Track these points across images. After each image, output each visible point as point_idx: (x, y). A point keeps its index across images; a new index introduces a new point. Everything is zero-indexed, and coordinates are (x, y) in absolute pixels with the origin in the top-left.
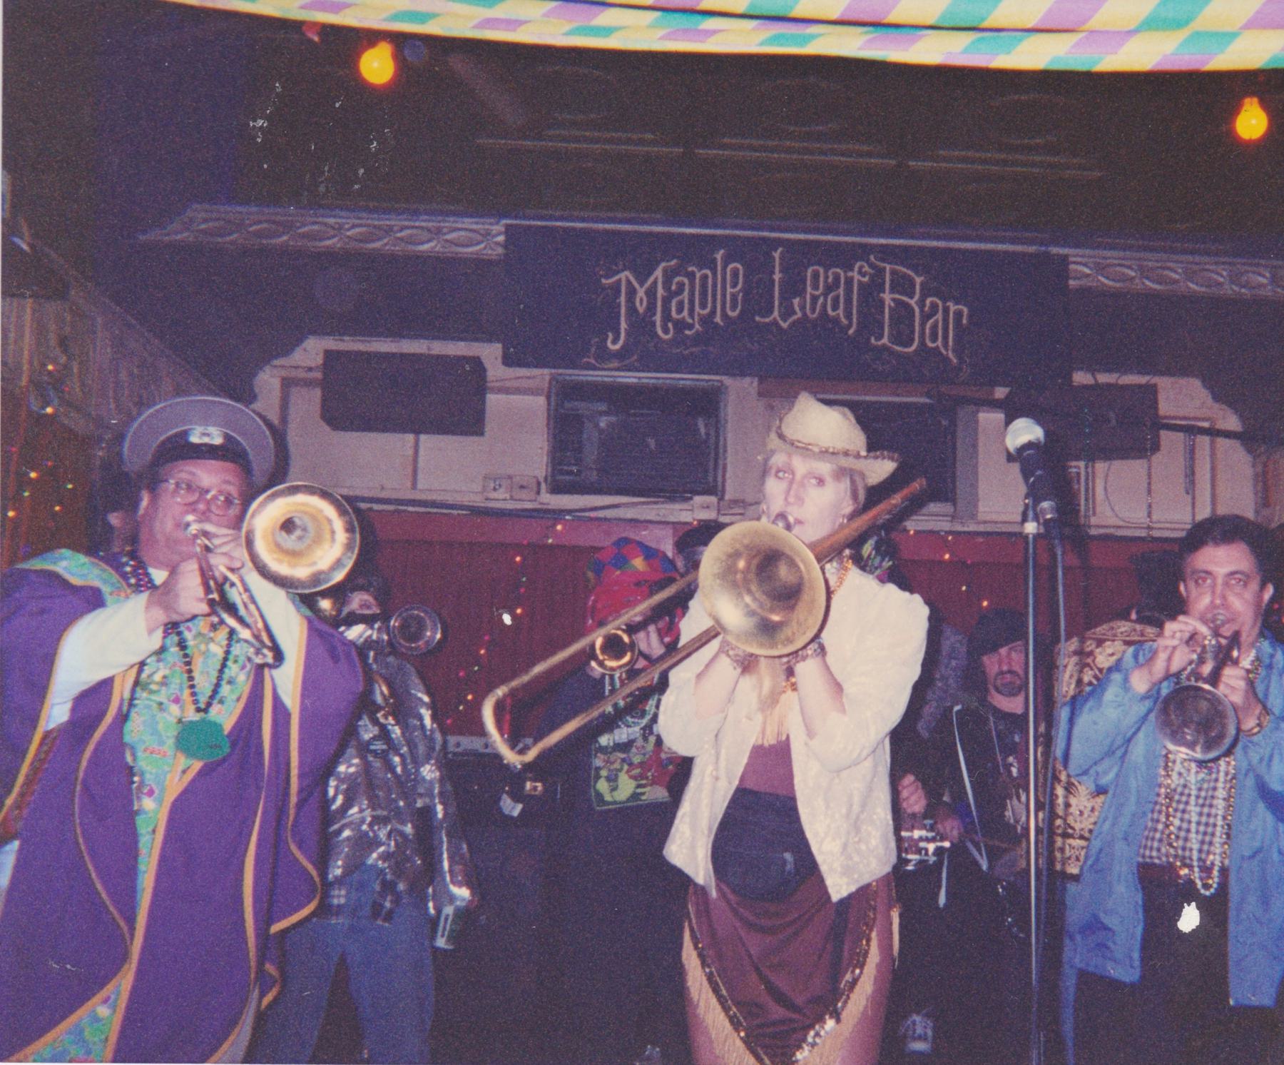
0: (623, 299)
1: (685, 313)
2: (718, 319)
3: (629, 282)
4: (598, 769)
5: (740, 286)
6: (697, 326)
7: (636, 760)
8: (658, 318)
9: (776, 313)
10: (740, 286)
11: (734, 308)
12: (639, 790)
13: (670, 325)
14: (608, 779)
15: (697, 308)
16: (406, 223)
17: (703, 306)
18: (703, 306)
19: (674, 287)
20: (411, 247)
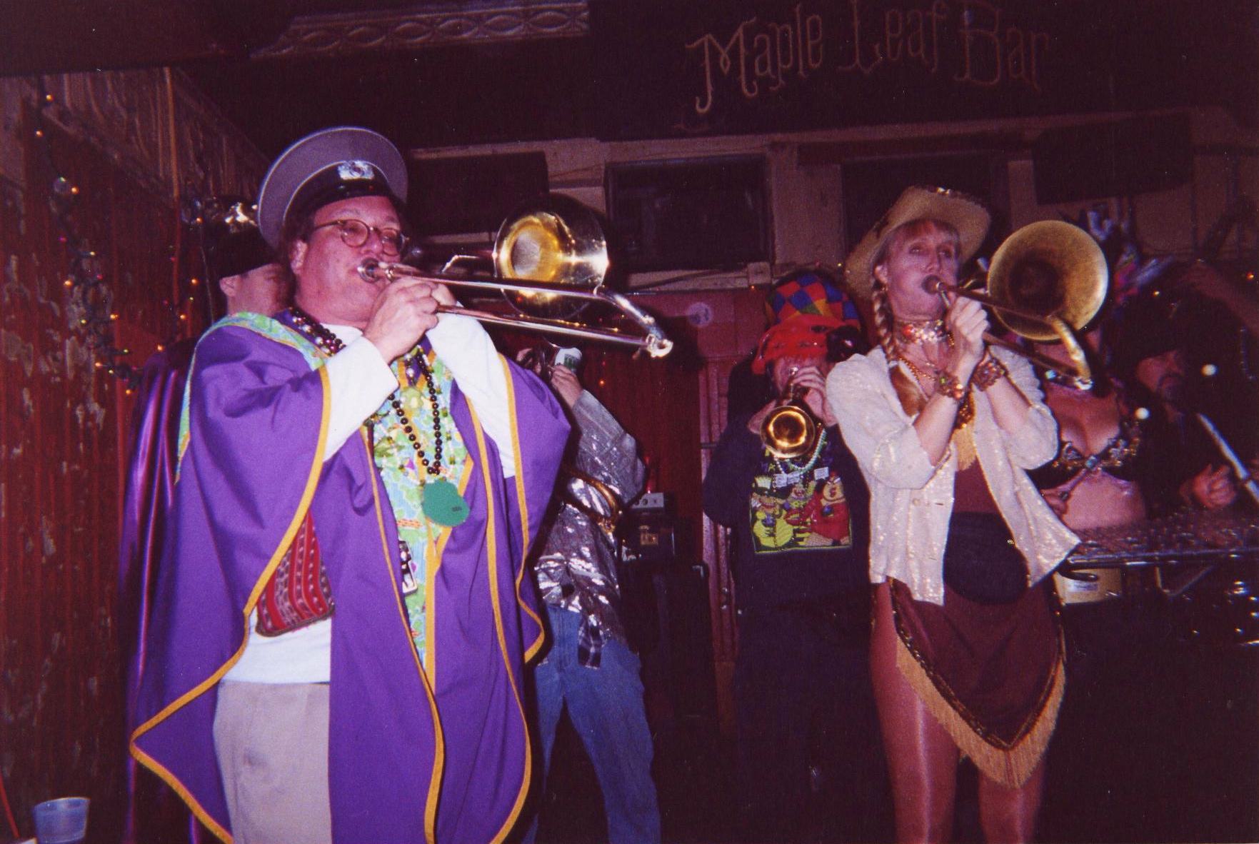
0: (707, 61)
1: (769, 70)
2: (801, 72)
3: (712, 47)
4: (755, 510)
5: (820, 38)
6: (781, 81)
7: (795, 505)
8: (743, 78)
9: (858, 61)
10: (820, 38)
11: (816, 60)
12: (799, 535)
13: (755, 83)
14: (765, 523)
15: (780, 65)
16: (492, 10)
17: (785, 60)
18: (785, 60)
19: (756, 44)
20: (499, 34)
